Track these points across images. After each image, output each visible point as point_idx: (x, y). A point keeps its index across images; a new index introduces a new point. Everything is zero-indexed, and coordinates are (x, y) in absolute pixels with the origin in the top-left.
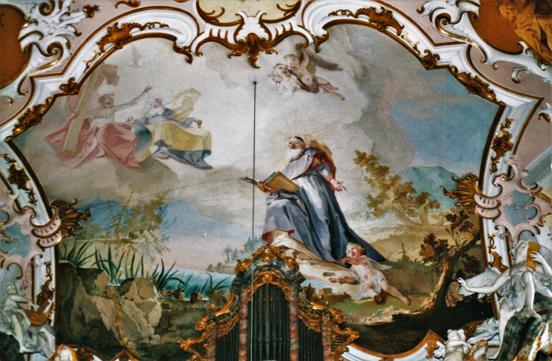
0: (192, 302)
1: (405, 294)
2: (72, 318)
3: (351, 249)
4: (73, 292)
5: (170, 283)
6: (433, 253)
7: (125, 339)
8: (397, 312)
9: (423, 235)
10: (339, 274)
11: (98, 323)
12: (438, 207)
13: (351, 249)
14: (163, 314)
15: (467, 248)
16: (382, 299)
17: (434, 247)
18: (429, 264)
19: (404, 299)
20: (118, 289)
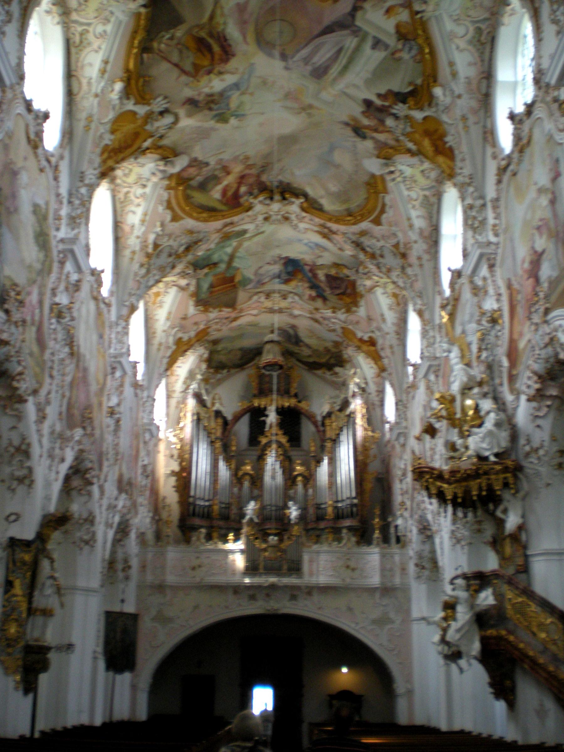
10: (297, 348)
16: (310, 356)
17: (327, 350)
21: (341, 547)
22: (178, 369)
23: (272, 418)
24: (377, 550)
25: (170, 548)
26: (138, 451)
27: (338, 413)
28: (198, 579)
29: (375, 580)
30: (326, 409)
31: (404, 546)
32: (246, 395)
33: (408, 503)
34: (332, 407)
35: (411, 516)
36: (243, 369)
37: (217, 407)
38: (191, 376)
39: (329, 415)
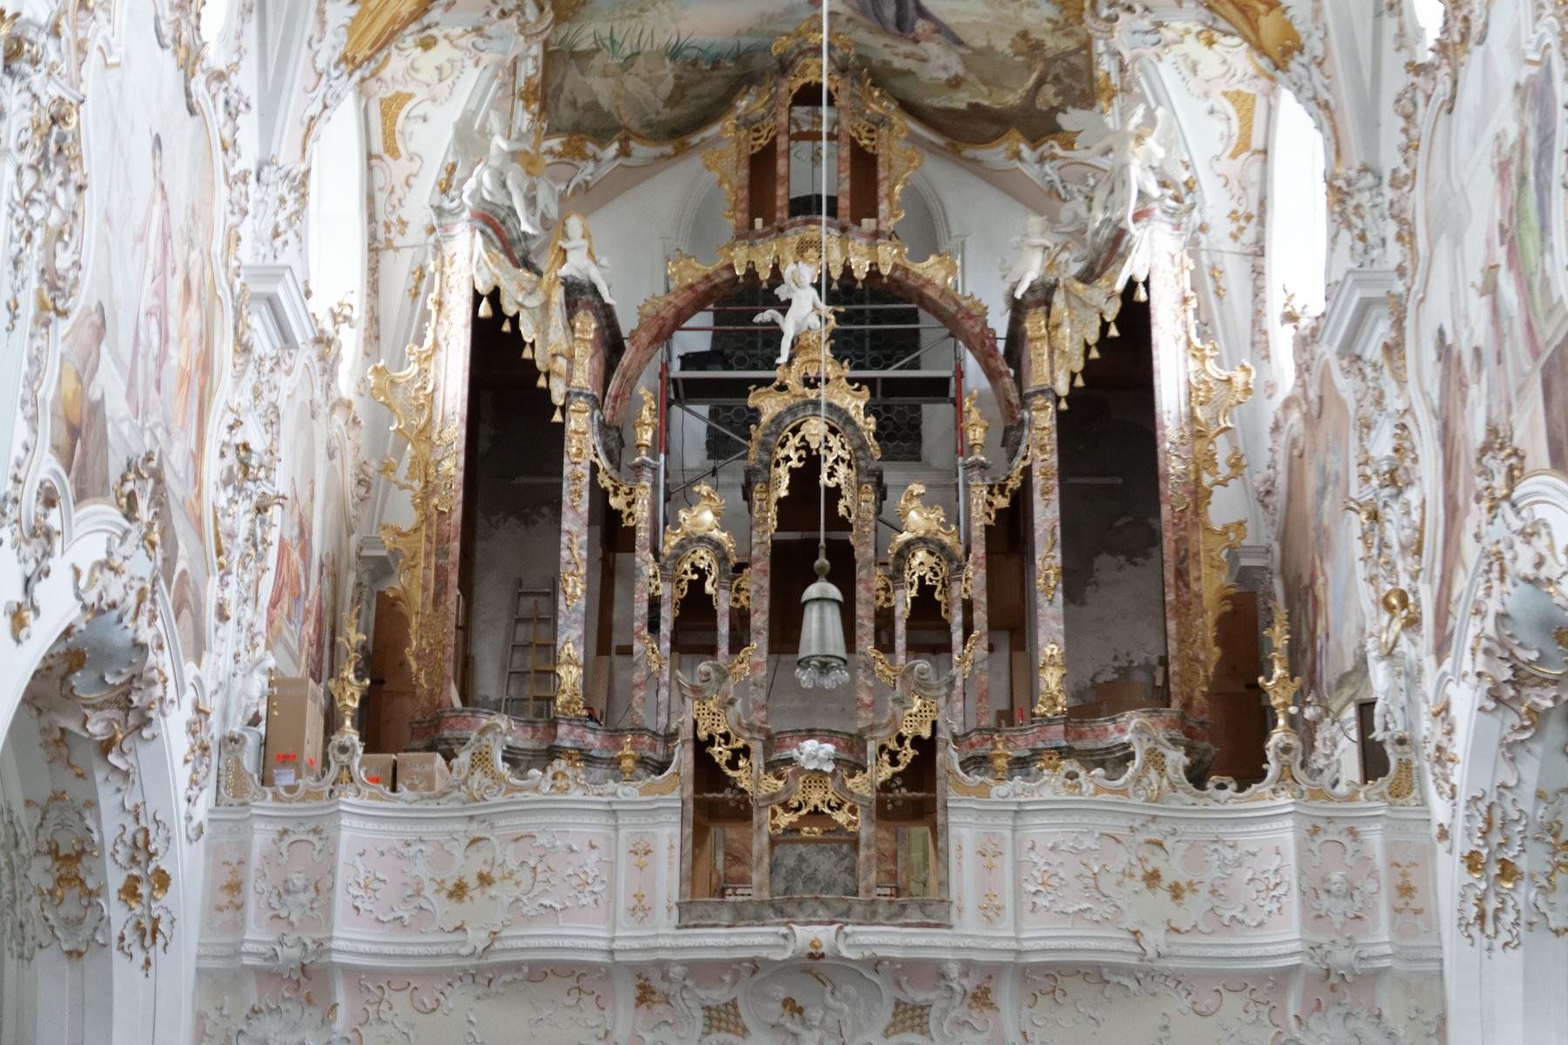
0: (713, 69)
1: (985, 83)
2: (561, 104)
3: (921, 25)
4: (564, 77)
5: (686, 52)
6: (1025, 49)
7: (626, 120)
8: (974, 101)
9: (1015, 29)
11: (593, 106)
12: (1037, 7)
13: (921, 25)
14: (676, 86)
15: (1071, 53)
16: (955, 83)
17: (1029, 46)
18: (1020, 59)
19: (985, 90)
20: (621, 65)
21: (1123, 791)
22: (416, 128)
23: (805, 313)
24: (1285, 800)
25: (348, 799)
26: (206, 364)
27: (1080, 286)
28: (477, 938)
29: (1282, 937)
30: (1032, 271)
31: (1397, 792)
32: (699, 230)
33: (1426, 598)
34: (1051, 265)
35: (1442, 647)
36: (682, 150)
37: (577, 265)
38: (469, 139)
39: (1043, 295)
